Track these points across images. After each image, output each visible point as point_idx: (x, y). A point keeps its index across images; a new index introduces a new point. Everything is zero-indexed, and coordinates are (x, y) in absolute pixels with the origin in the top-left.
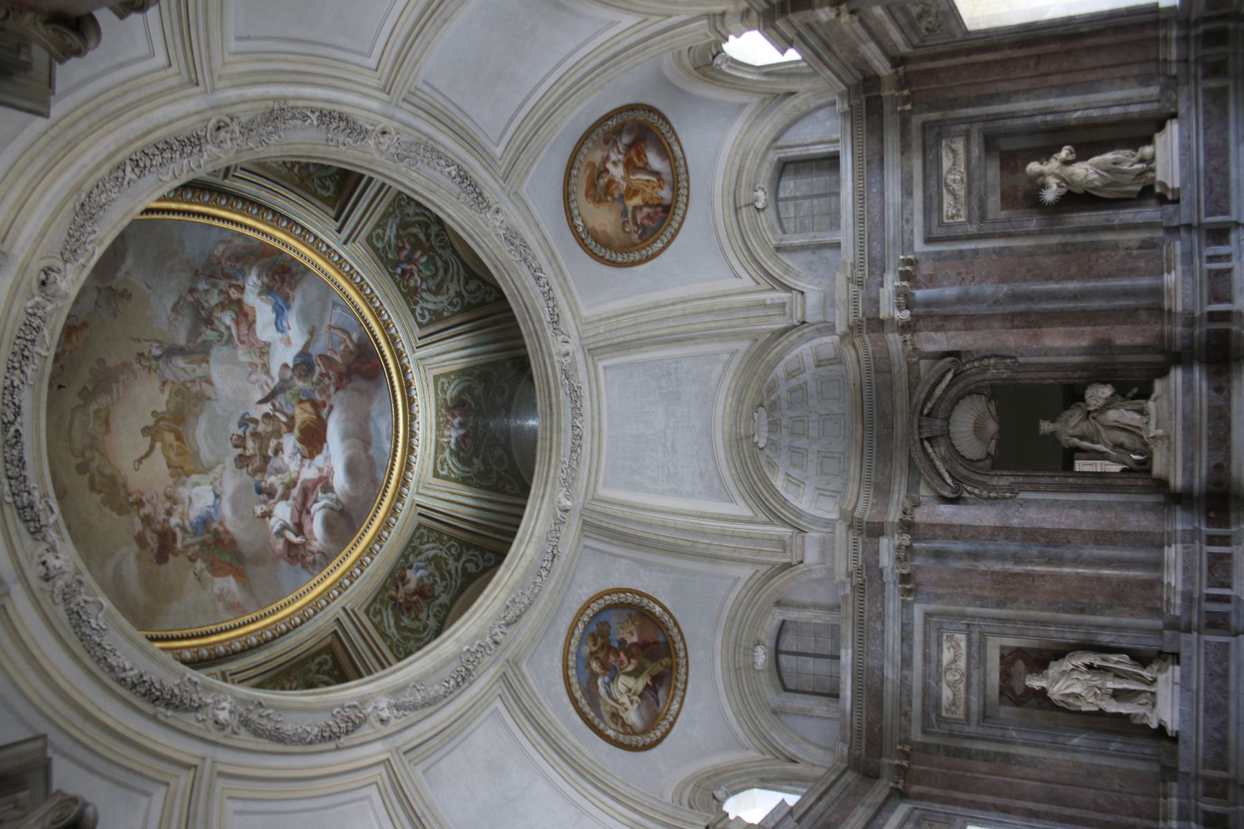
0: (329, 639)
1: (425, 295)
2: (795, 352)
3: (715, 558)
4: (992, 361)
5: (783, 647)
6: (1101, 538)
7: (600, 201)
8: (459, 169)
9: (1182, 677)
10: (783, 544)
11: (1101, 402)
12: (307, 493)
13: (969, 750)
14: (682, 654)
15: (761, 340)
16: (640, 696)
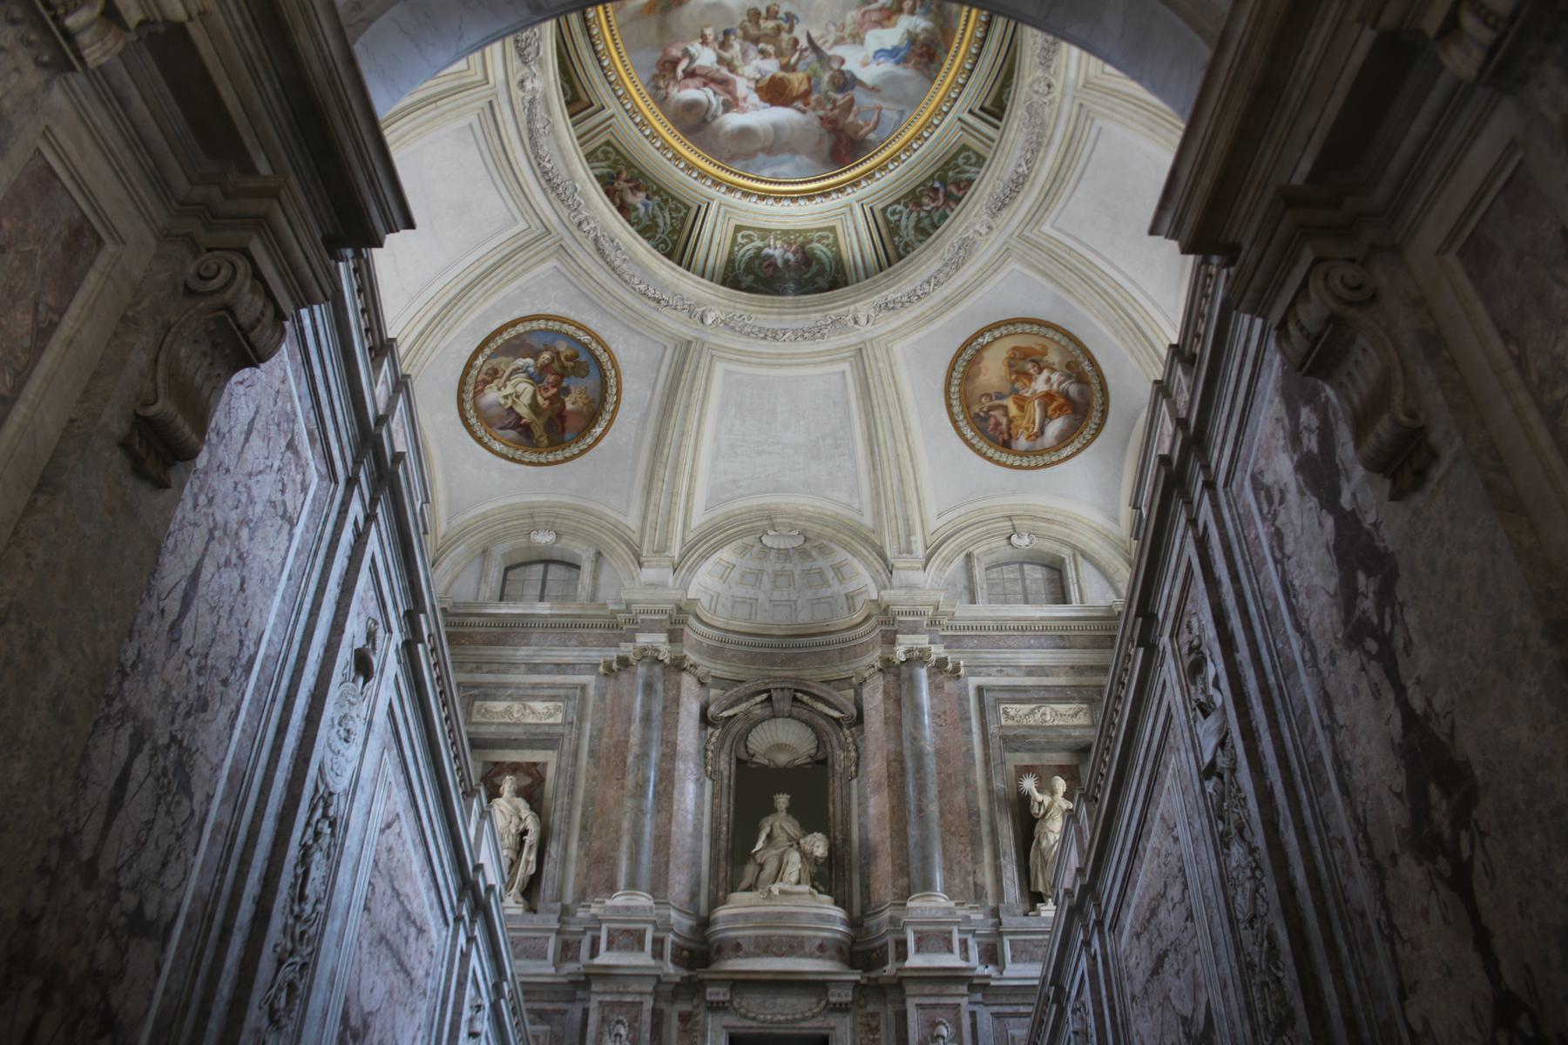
0: (585, 98)
1: (914, 215)
2: (861, 568)
3: (648, 490)
4: (853, 754)
5: (552, 568)
6: (663, 841)
7: (1010, 366)
8: (1026, 176)
9: (510, 916)
10: (661, 550)
11: (807, 847)
12: (724, 84)
14: (551, 457)
15: (873, 537)
16: (511, 408)
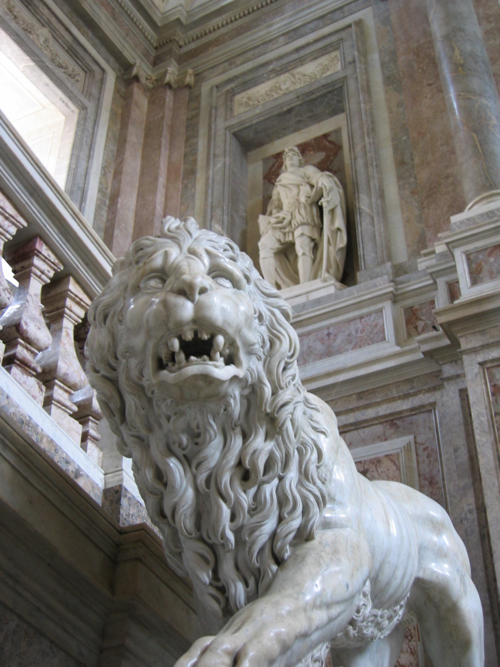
9: (318, 301)
13: (196, 136)
